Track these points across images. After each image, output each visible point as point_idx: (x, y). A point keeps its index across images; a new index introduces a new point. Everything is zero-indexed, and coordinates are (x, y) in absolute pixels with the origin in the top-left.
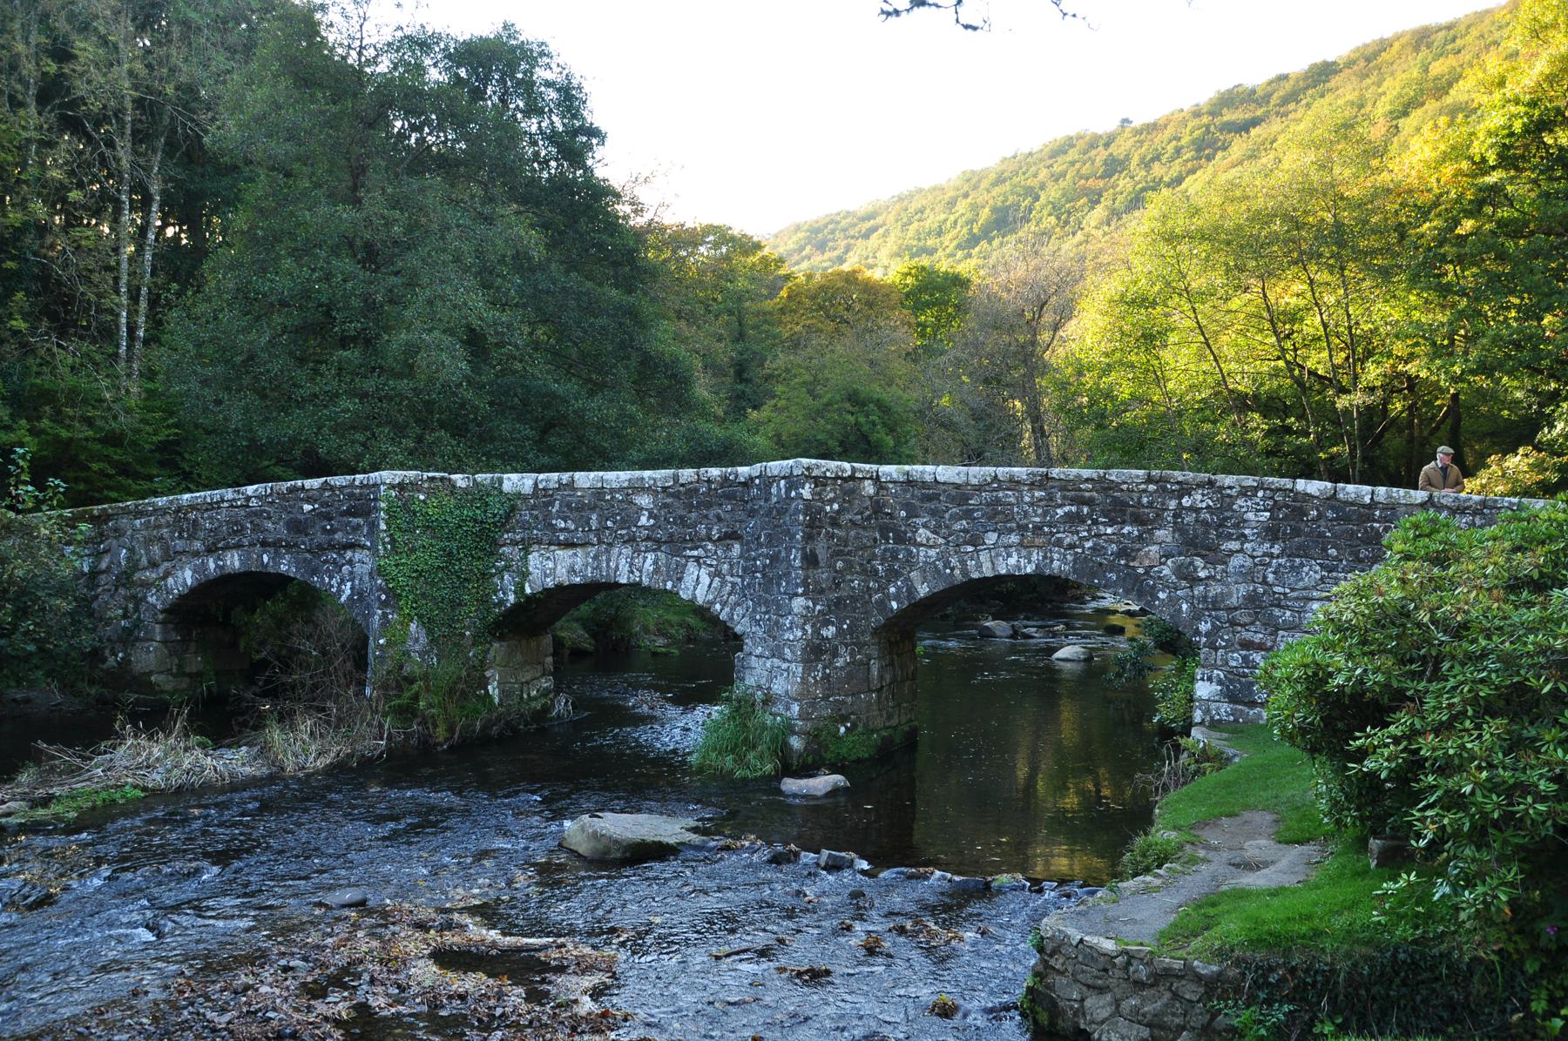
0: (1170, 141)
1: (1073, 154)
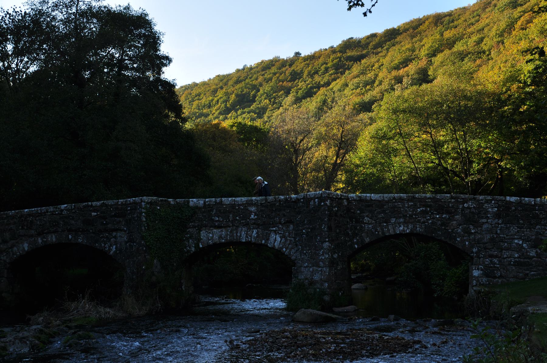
0: (322, 65)
1: (274, 69)
